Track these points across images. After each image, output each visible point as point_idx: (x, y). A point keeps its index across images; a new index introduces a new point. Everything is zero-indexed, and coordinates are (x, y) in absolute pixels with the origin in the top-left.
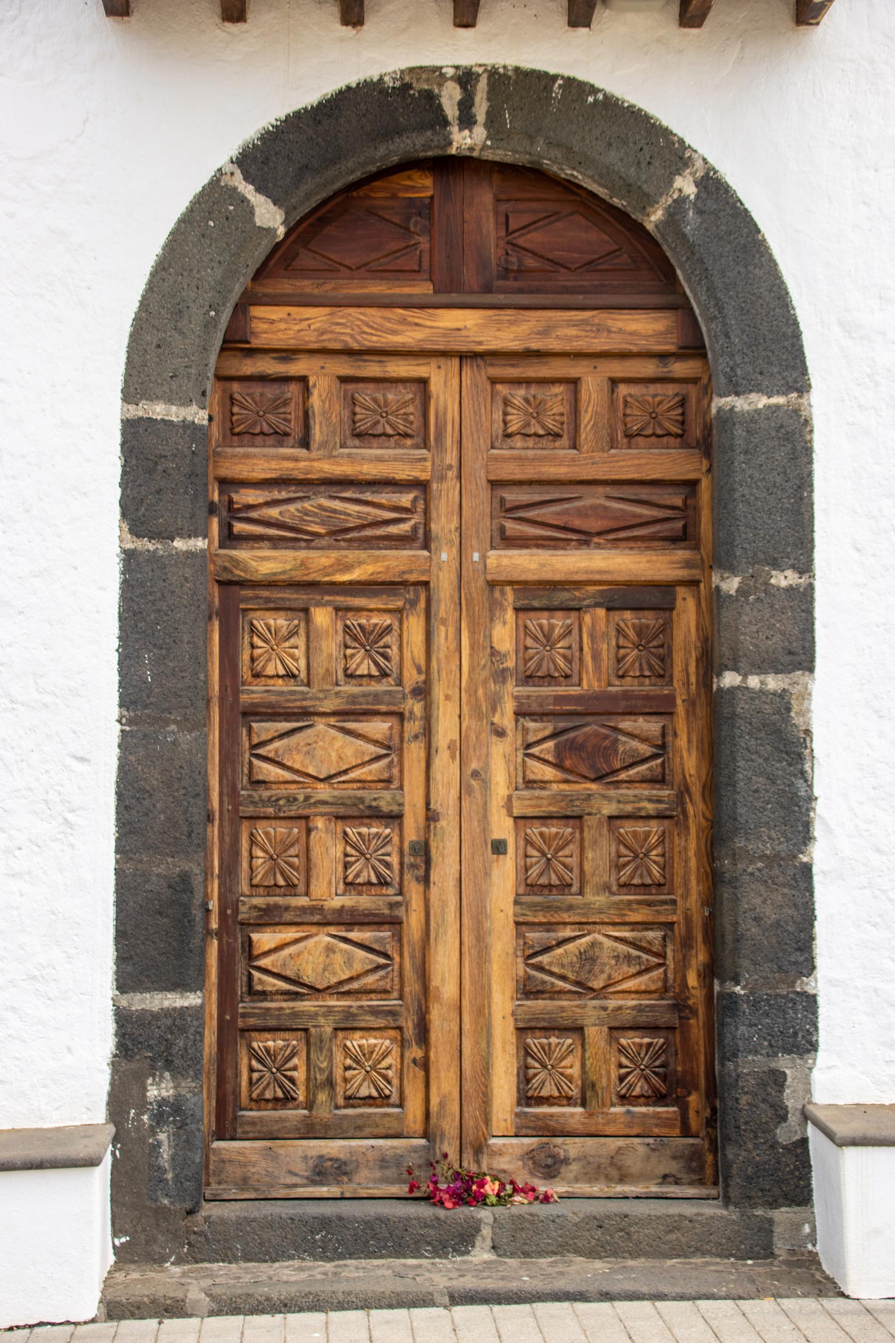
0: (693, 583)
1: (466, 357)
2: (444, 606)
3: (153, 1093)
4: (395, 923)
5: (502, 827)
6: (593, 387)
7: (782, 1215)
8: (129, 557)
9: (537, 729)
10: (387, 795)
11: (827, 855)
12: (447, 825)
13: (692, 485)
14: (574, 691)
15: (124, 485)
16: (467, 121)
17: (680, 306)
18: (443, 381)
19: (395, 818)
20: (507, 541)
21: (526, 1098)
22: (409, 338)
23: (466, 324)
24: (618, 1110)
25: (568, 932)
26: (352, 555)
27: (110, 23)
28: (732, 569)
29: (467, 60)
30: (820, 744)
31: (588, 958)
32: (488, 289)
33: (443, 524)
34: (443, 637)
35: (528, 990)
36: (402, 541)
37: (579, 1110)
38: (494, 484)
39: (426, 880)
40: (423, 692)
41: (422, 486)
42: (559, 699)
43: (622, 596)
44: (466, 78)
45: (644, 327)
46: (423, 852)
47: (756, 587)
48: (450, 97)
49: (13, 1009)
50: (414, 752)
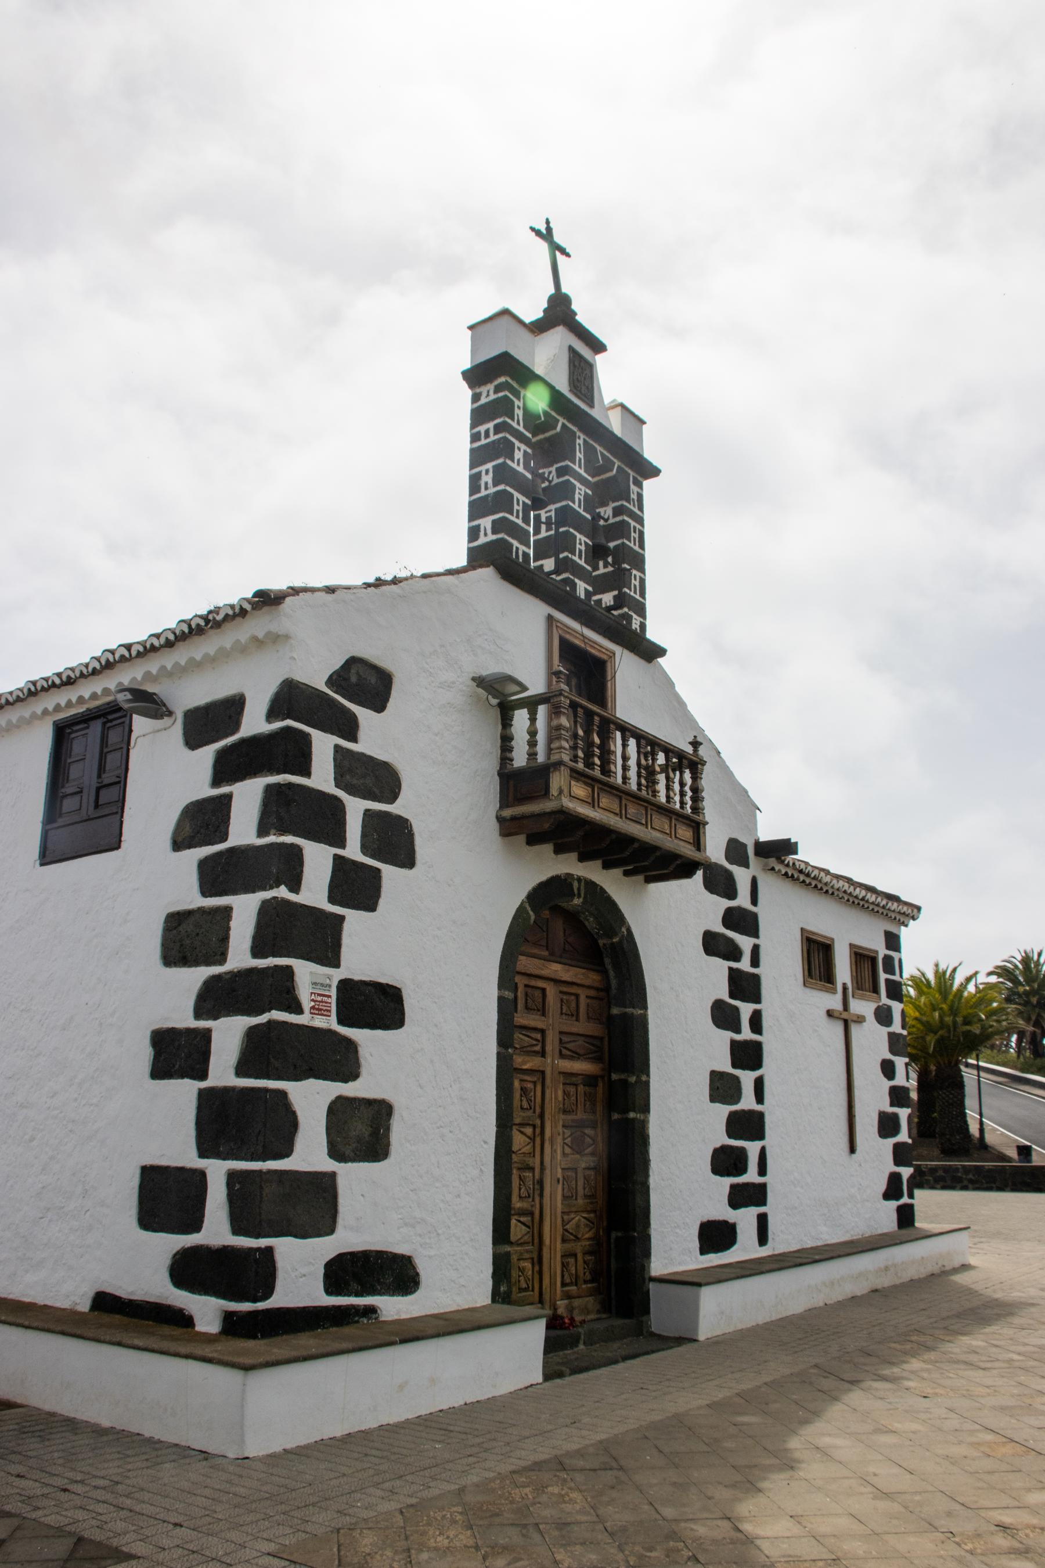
0: (602, 1077)
1: (556, 981)
2: (548, 1081)
3: (502, 1289)
4: (532, 1214)
5: (560, 1176)
6: (583, 1000)
7: (644, 1318)
8: (498, 1054)
9: (568, 1132)
10: (531, 1159)
11: (653, 1181)
12: (548, 1172)
13: (601, 1039)
14: (575, 1117)
15: (498, 1024)
16: (579, 896)
17: (604, 972)
18: (551, 991)
19: (532, 1169)
20: (562, 1056)
21: (563, 1284)
22: (544, 972)
23: (556, 969)
24: (584, 1286)
25: (572, 1216)
26: (527, 1058)
27: (499, 838)
28: (633, 1074)
29: (580, 873)
30: (652, 1140)
31: (578, 1226)
32: (561, 957)
33: (549, 1048)
34: (548, 1092)
35: (564, 1241)
36: (536, 1053)
37: (575, 1288)
38: (561, 1033)
39: (541, 1195)
40: (542, 1116)
41: (543, 1032)
42: (573, 1121)
43: (590, 1081)
44: (579, 879)
45: (593, 978)
46: (541, 1182)
47: (638, 1081)
48: (576, 884)
49: (467, 1254)
50: (538, 1140)
